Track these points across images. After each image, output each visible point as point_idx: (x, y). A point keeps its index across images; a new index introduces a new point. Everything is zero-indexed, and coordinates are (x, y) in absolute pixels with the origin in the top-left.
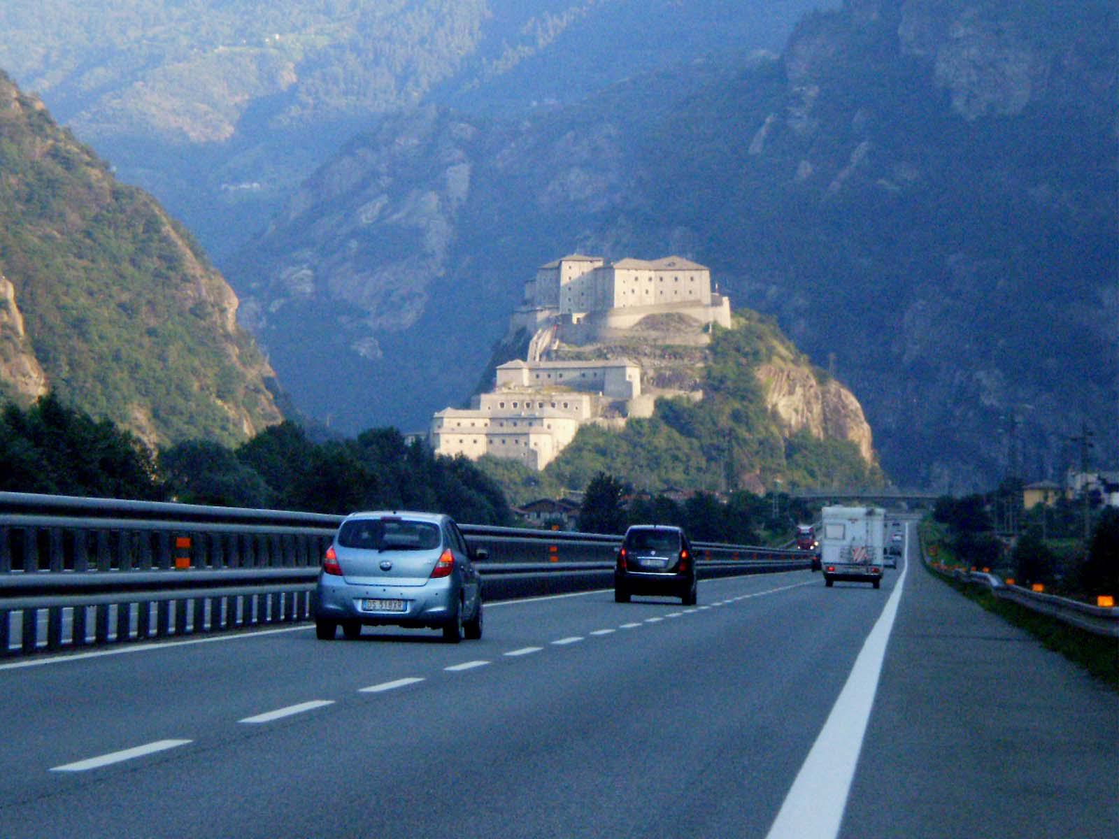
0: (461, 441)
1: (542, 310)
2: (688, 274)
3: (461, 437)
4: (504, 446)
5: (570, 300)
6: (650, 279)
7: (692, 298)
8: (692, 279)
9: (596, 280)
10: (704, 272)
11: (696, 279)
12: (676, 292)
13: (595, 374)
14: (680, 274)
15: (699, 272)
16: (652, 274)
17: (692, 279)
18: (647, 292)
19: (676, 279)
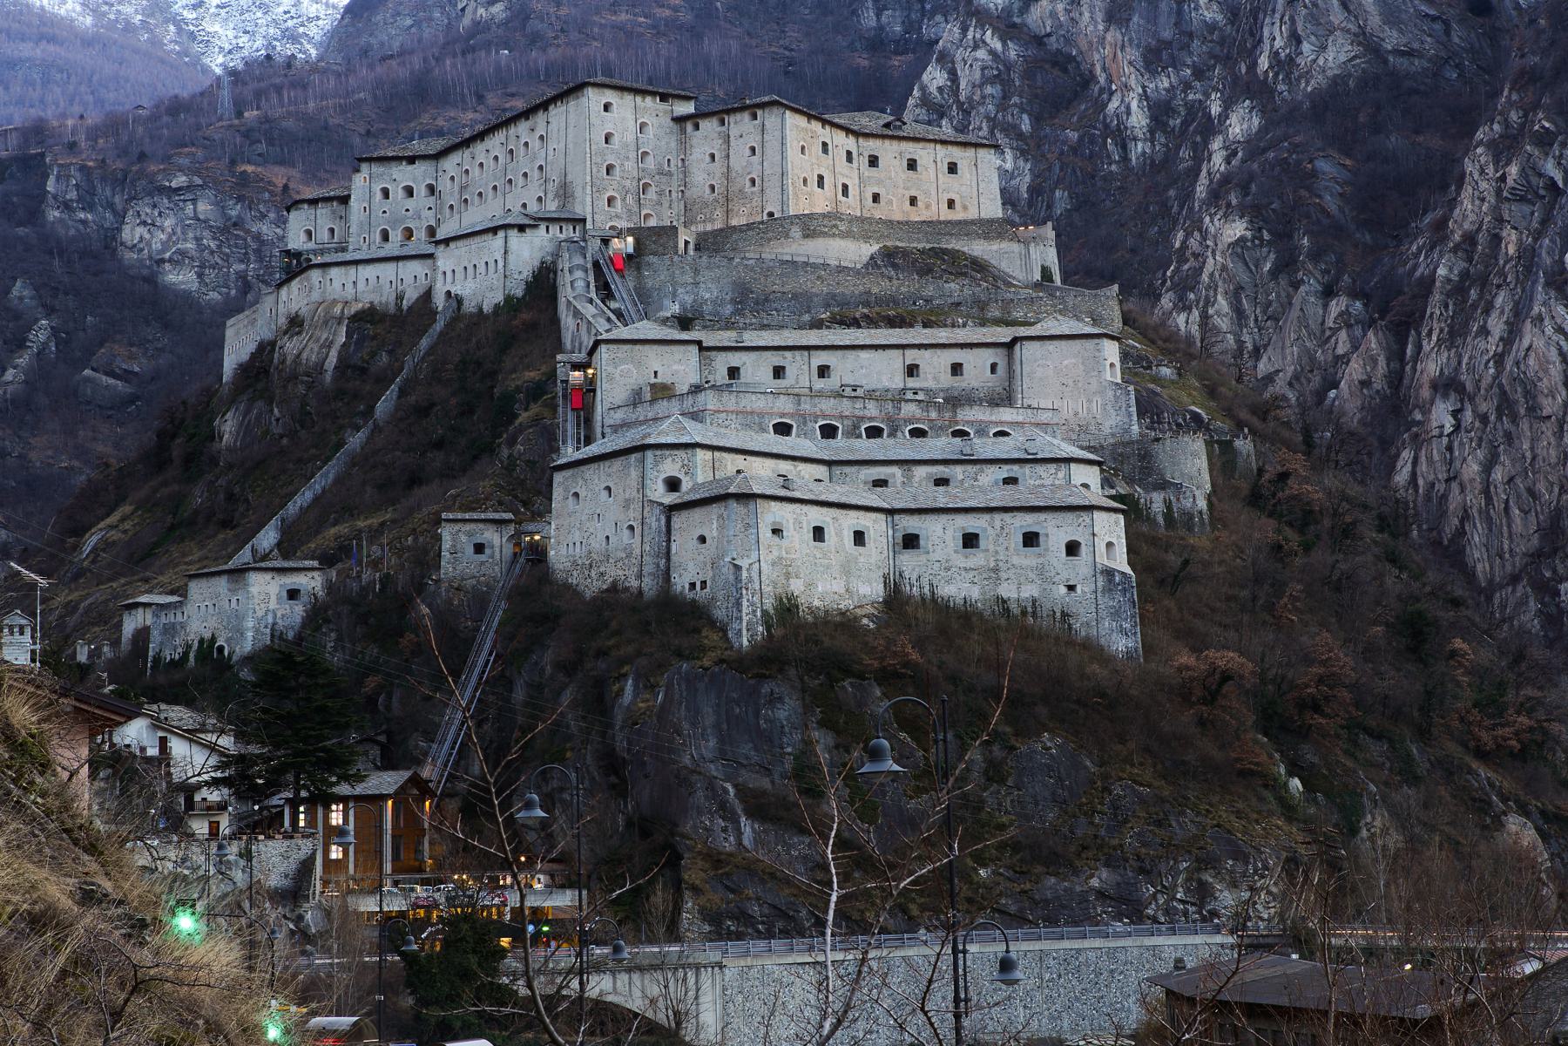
0: (818, 533)
1: (522, 228)
2: (945, 154)
3: (817, 516)
4: (976, 559)
5: (610, 200)
6: (849, 153)
7: (958, 215)
8: (952, 169)
9: (684, 145)
10: (982, 152)
11: (963, 167)
12: (913, 201)
13: (956, 369)
14: (923, 153)
15: (970, 152)
16: (850, 143)
17: (952, 169)
18: (845, 188)
19: (912, 165)
